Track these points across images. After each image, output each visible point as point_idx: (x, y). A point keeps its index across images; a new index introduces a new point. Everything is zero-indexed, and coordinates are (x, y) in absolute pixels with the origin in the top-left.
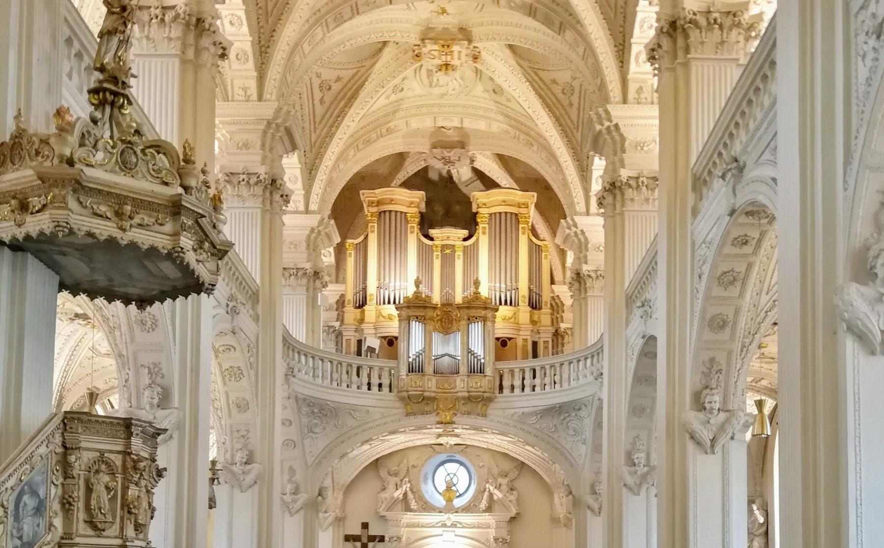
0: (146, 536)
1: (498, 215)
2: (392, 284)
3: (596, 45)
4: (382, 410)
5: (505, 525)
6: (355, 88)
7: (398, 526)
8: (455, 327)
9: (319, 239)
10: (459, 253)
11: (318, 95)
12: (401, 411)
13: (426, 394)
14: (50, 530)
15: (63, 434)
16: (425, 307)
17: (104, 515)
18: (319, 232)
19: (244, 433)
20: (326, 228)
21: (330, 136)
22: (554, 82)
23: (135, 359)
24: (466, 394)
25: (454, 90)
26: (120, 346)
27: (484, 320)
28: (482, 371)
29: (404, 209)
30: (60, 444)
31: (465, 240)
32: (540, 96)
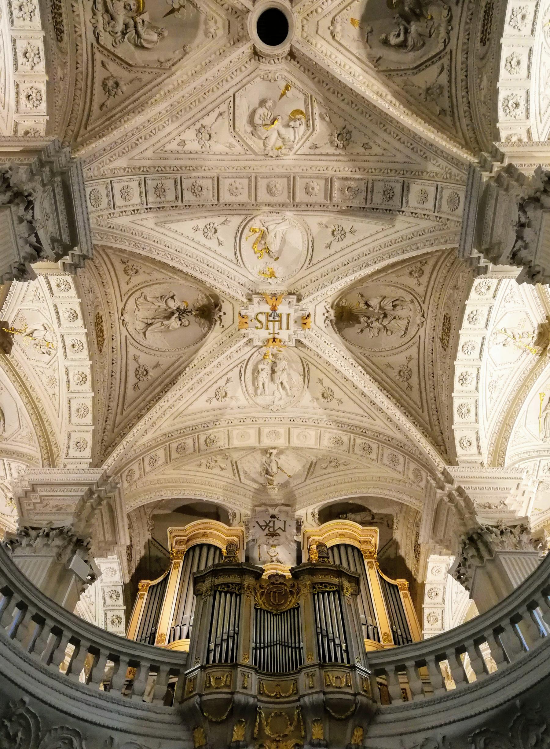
6: (174, 374)
22: (389, 366)
25: (280, 399)
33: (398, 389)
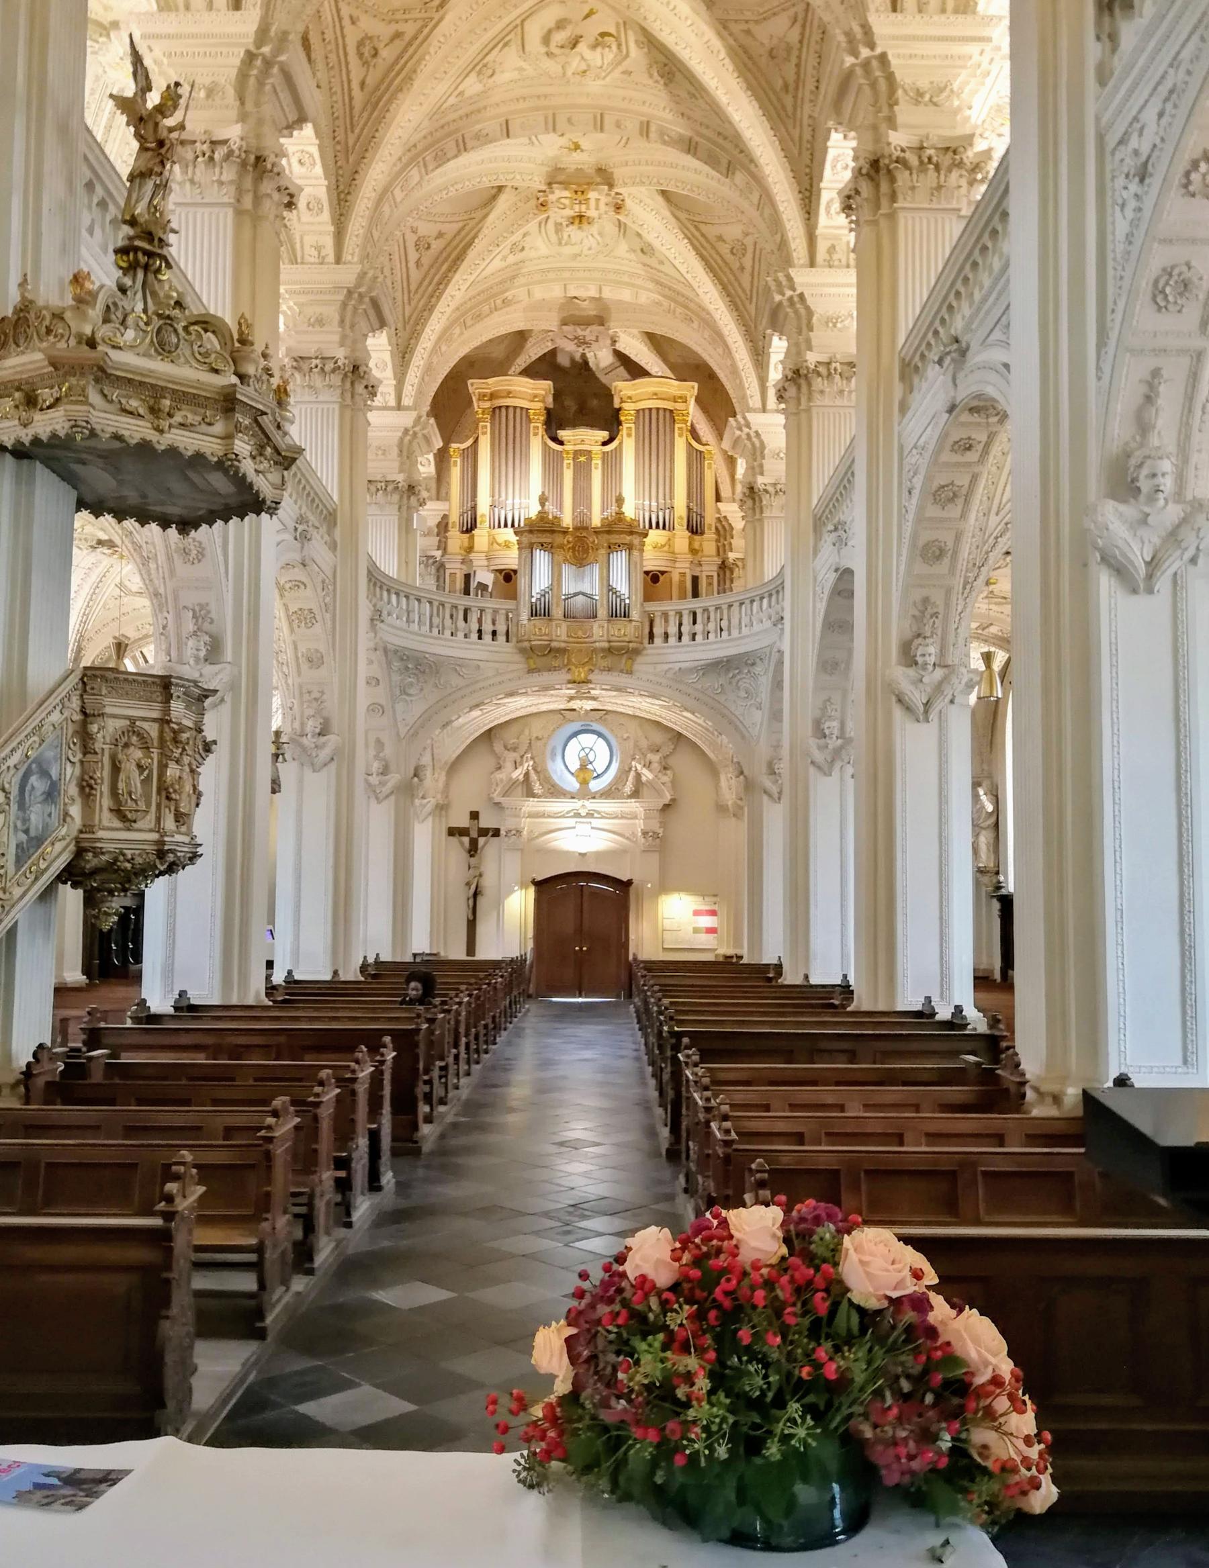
0: (190, 828)
1: (647, 412)
2: (510, 501)
3: (775, 191)
4: (497, 665)
5: (657, 814)
6: (461, 246)
7: (517, 816)
8: (591, 558)
9: (415, 443)
10: (597, 462)
11: (413, 256)
12: (521, 666)
13: (554, 644)
14: (64, 821)
15: (82, 696)
16: (553, 532)
17: (136, 801)
18: (415, 434)
19: (318, 695)
20: (423, 429)
21: (429, 308)
22: (720, 238)
23: (176, 599)
24: (606, 645)
25: (590, 249)
26: (156, 582)
27: (630, 548)
28: (626, 615)
29: (525, 404)
30: (78, 709)
31: (605, 444)
32: (702, 257)
33: (726, 270)
